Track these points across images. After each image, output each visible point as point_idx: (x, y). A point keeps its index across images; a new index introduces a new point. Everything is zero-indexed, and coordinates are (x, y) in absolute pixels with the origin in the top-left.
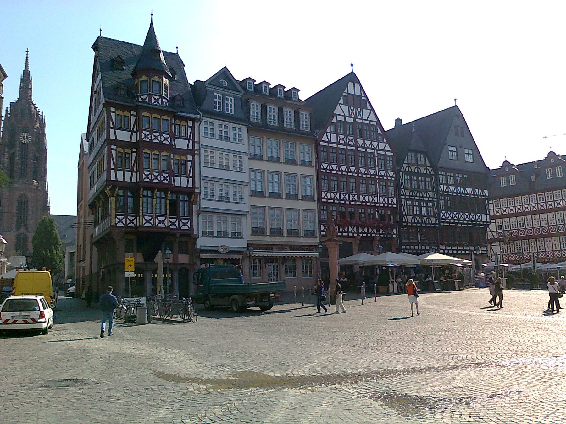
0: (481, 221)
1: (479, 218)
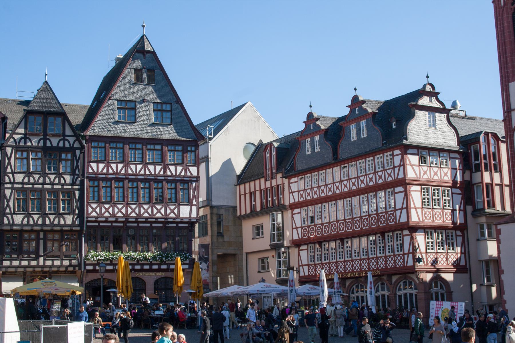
0: (178, 216)
1: (172, 211)
